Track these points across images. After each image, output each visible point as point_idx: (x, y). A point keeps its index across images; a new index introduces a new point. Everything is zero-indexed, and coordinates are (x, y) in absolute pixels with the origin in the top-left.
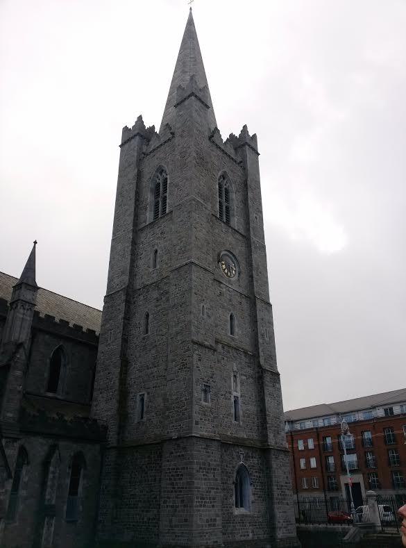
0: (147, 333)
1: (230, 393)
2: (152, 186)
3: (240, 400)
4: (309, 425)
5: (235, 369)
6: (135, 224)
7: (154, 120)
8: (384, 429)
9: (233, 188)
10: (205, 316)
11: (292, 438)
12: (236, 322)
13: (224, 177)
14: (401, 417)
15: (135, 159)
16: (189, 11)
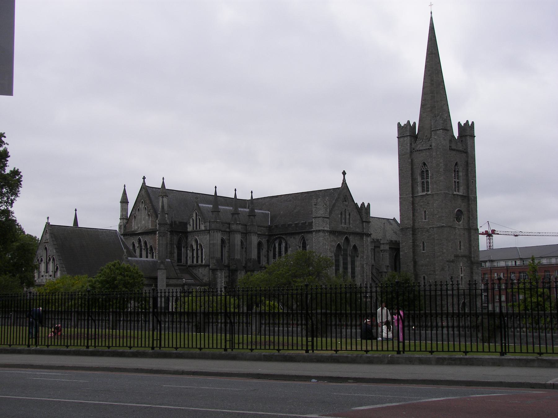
0: (424, 250)
1: (460, 276)
2: (419, 172)
3: (463, 278)
4: (502, 264)
5: (461, 266)
6: (413, 194)
7: (414, 117)
8: (545, 271)
9: (461, 169)
10: (450, 249)
11: (491, 271)
12: (462, 244)
13: (456, 164)
14: (555, 265)
15: (409, 151)
16: (430, 14)
